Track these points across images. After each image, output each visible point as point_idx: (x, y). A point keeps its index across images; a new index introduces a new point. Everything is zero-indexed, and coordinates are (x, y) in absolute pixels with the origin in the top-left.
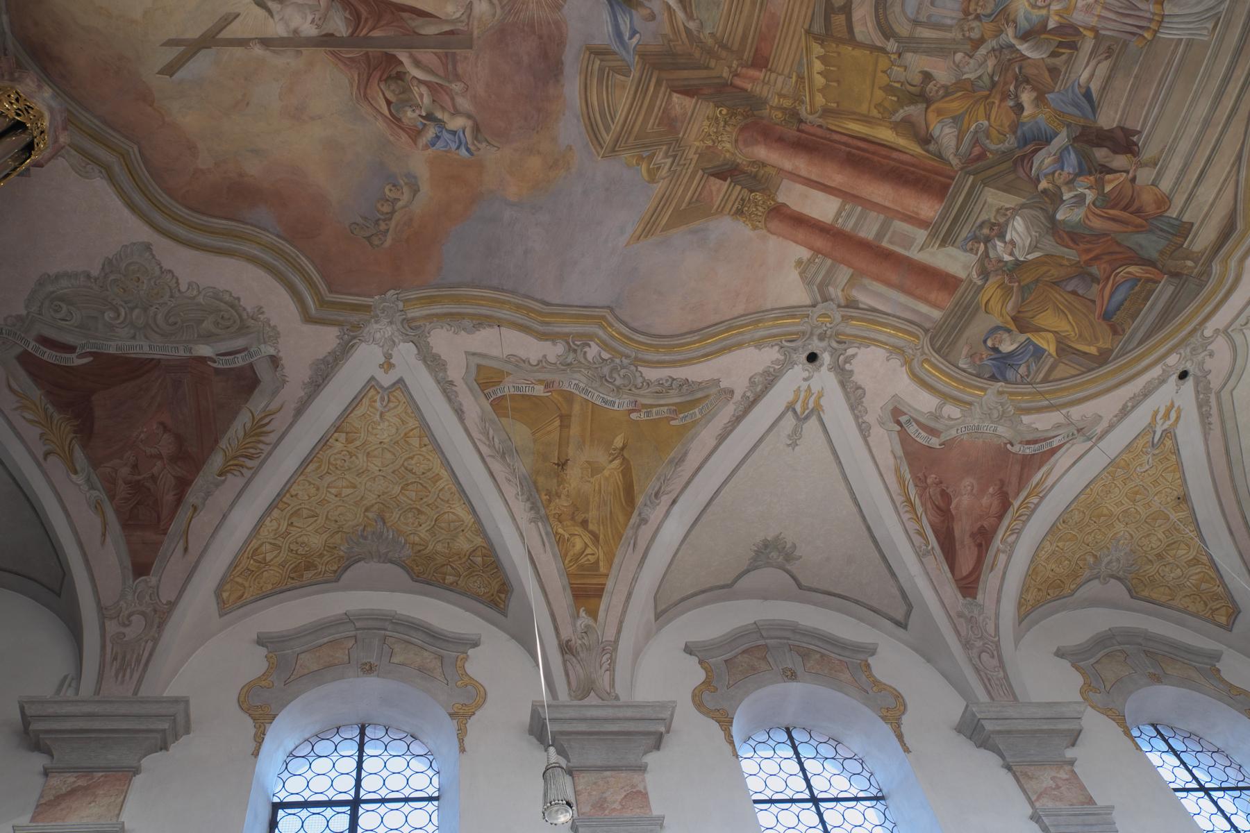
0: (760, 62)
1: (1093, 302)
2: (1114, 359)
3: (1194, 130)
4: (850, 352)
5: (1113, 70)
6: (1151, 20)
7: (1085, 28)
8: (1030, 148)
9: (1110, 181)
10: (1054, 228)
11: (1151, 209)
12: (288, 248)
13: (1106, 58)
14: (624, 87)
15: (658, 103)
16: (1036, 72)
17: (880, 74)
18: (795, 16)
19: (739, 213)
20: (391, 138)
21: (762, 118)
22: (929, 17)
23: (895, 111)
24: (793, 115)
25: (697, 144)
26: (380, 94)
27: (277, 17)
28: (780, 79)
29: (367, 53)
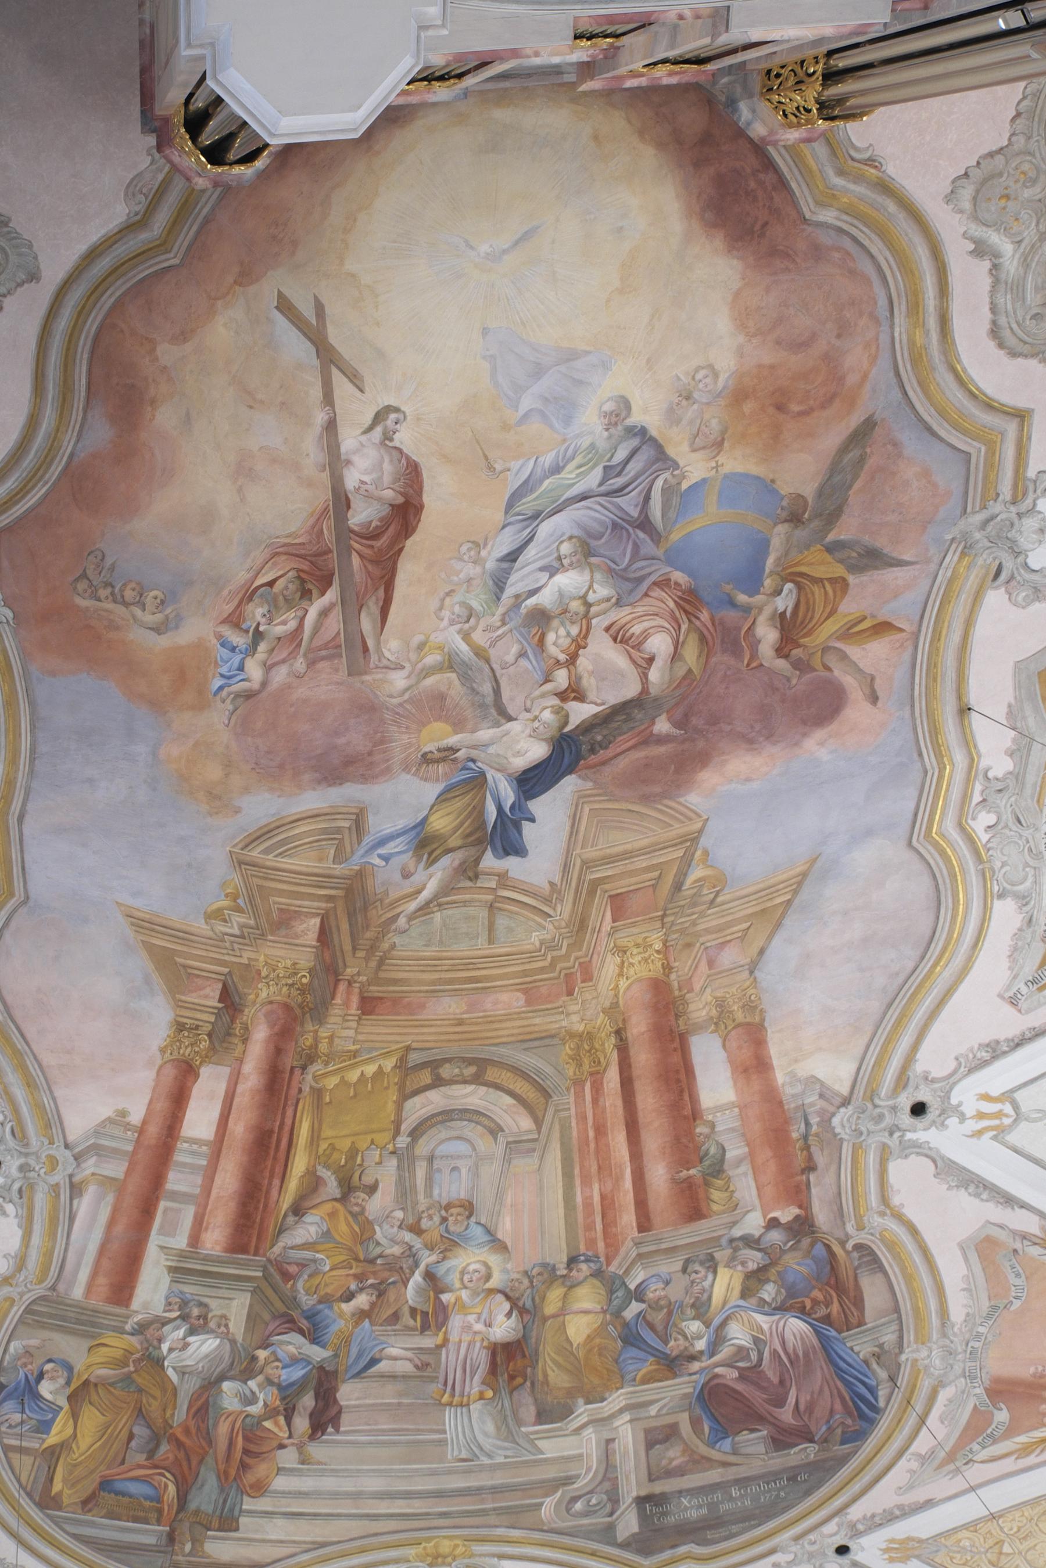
0: (368, 1005)
1: (123, 1463)
2: (48, 1516)
3: (348, 1485)
4: (10, 1208)
5: (405, 1377)
6: (462, 1395)
7: (446, 1333)
8: (304, 1324)
9: (276, 1424)
10: (211, 1384)
11: (250, 1478)
12: (56, 470)
13: (416, 1367)
14: (320, 860)
15: (306, 903)
16: (392, 1300)
17: (369, 1138)
18: (425, 1030)
19: (180, 1027)
20: (225, 592)
21: (302, 1024)
22: (439, 1170)
23: (327, 1167)
24: (310, 1058)
25: (262, 958)
26: (282, 573)
27: (364, 438)
28: (351, 1033)
29: (331, 551)
